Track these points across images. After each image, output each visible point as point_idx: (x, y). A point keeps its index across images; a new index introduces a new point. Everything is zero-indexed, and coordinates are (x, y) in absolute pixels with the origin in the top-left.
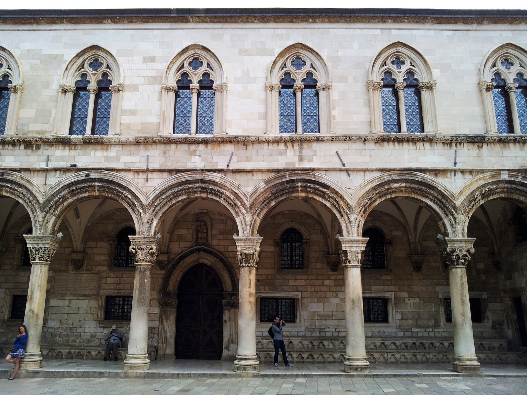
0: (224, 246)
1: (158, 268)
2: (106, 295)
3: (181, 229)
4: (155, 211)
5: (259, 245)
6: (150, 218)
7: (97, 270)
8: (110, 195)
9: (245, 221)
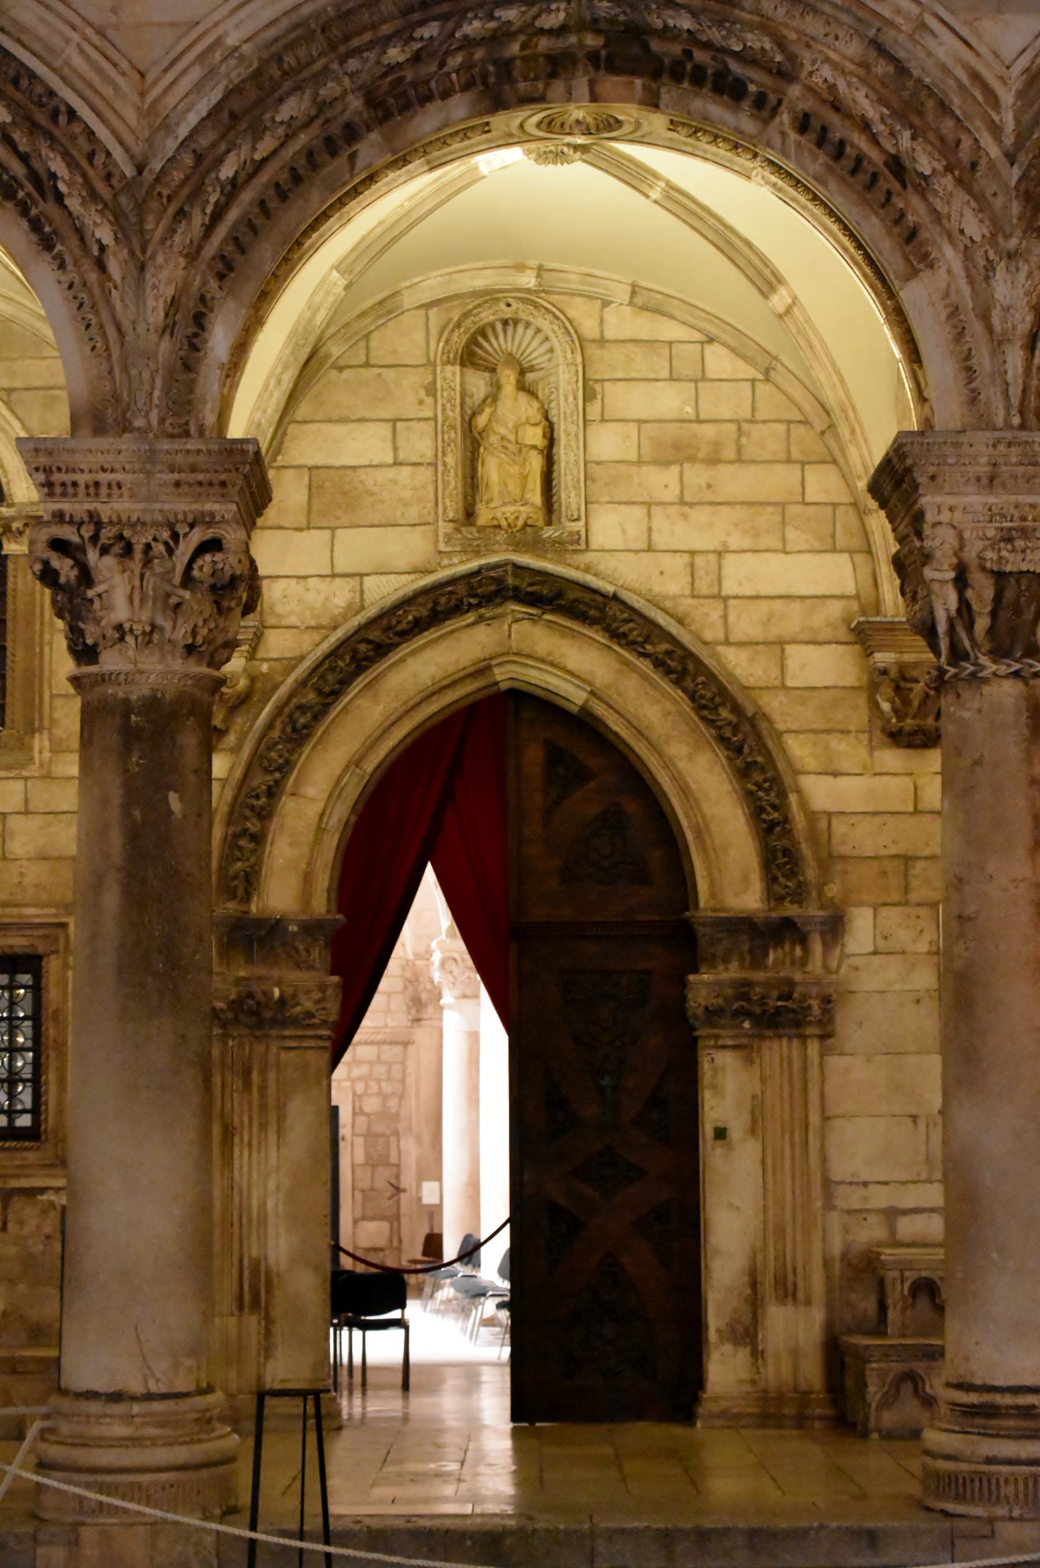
0: (692, 553)
3: (339, 430)
4: (221, 232)
6: (183, 289)
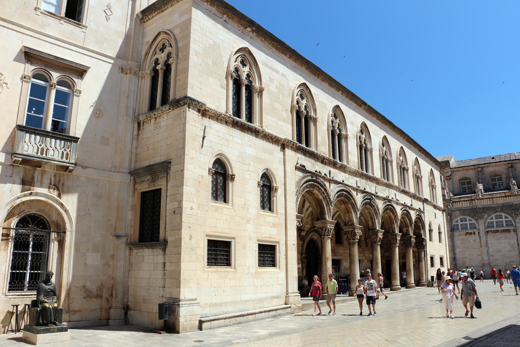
5: (382, 234)
8: (347, 200)
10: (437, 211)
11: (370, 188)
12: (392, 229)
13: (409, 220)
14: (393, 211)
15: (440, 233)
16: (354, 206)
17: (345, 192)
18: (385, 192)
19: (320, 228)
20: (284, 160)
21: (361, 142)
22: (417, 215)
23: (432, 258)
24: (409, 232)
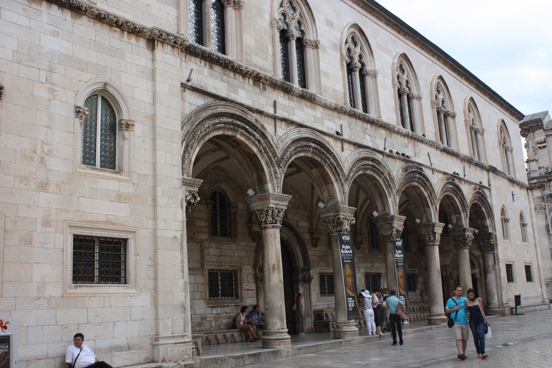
1: (251, 240)
2: (209, 269)
5: (403, 223)
7: (199, 238)
9: (395, 201)
10: (516, 189)
11: (372, 141)
12: (427, 217)
13: (459, 201)
14: (426, 184)
15: (523, 225)
16: (336, 170)
17: (313, 142)
18: (406, 149)
19: (258, 210)
20: (153, 70)
21: (351, 58)
22: (476, 193)
23: (509, 268)
24: (461, 221)
